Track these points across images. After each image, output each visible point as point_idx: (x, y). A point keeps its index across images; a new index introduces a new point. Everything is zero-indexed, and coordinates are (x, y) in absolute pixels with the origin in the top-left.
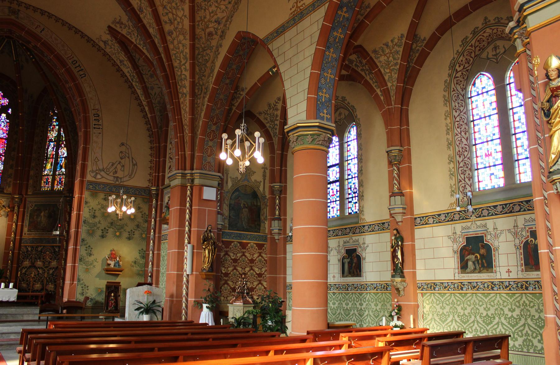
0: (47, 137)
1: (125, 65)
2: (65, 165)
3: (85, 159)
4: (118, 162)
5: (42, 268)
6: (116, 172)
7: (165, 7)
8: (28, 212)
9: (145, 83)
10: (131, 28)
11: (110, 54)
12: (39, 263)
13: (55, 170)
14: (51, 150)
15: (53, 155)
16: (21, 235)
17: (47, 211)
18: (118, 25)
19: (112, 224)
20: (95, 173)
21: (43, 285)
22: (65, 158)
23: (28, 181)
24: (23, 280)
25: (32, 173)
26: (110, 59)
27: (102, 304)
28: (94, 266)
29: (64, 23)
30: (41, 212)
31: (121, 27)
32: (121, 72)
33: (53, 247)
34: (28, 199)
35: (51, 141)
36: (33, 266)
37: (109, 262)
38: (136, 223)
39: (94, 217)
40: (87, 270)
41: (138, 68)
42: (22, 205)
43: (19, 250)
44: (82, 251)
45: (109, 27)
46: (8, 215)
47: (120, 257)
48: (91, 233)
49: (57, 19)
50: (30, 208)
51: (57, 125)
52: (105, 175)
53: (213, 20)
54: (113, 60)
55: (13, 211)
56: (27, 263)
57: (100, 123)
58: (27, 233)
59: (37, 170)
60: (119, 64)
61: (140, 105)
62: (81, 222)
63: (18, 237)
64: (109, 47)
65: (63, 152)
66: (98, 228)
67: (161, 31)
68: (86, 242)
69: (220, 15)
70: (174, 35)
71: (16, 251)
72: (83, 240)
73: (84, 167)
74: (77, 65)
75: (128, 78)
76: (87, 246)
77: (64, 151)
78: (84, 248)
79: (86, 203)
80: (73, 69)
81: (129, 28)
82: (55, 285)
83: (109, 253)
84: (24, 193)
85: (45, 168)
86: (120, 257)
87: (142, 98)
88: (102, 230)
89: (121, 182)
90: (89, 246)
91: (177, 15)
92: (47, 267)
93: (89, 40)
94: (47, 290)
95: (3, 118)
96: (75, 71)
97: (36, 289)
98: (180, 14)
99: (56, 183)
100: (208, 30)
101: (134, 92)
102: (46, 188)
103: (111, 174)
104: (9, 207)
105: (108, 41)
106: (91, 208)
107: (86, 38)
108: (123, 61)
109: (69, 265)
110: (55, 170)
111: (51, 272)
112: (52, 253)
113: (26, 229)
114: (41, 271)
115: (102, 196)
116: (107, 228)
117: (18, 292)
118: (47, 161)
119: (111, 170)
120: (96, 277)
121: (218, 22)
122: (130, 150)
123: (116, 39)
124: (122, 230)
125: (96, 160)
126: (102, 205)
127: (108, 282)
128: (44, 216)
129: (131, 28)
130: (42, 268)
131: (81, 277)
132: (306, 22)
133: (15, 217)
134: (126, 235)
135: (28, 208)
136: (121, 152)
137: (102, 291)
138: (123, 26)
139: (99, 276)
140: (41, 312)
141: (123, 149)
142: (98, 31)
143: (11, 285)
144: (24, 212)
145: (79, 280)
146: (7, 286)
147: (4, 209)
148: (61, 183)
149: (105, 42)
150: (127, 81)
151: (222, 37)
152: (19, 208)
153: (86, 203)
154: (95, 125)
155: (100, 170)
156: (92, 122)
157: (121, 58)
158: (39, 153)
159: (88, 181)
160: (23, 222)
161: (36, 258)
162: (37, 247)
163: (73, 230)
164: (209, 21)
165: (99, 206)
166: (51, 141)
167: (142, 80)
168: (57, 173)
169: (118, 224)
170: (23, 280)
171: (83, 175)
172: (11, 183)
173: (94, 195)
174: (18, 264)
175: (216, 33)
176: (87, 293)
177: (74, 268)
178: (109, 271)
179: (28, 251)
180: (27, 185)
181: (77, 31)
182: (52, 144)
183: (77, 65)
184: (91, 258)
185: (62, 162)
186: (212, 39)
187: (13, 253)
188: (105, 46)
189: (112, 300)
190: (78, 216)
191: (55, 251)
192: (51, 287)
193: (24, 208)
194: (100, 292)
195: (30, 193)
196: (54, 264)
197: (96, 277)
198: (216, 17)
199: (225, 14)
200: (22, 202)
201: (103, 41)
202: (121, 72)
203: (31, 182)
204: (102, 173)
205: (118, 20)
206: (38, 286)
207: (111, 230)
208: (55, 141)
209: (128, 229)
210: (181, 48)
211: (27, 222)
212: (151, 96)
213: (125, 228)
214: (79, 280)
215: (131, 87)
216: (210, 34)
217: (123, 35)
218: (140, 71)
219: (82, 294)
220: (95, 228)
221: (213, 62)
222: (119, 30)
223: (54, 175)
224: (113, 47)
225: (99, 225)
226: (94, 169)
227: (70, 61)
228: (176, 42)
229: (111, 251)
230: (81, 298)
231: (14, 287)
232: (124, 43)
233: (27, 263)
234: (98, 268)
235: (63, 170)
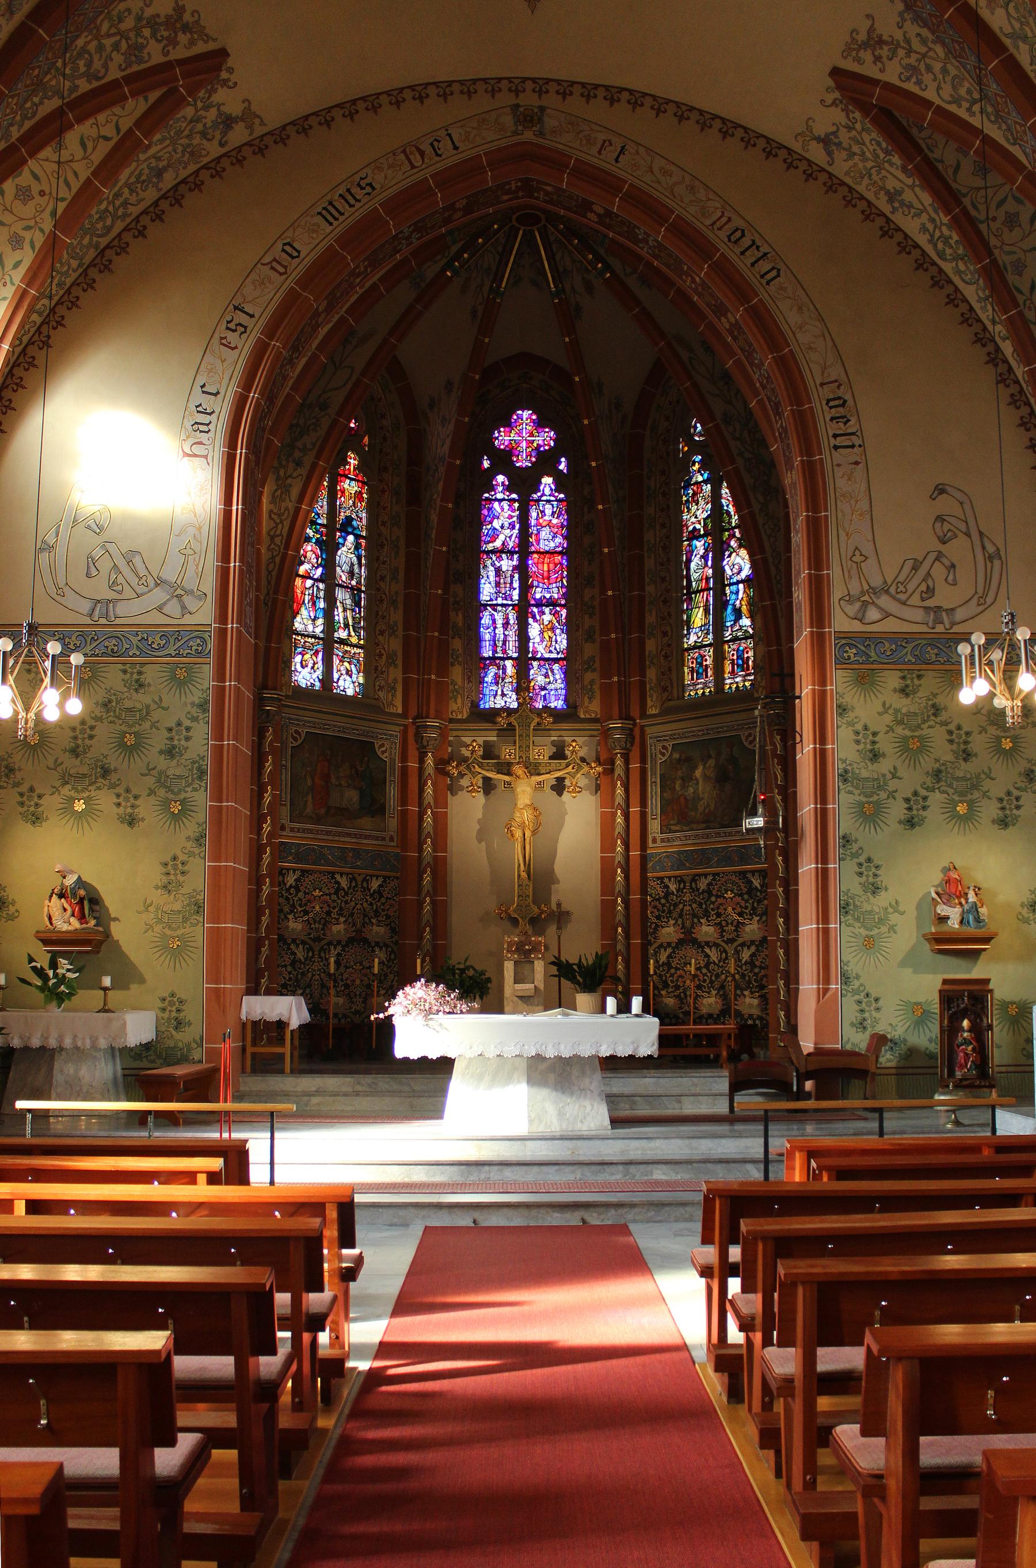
0: (681, 525)
1: (910, 206)
2: (749, 604)
3: (818, 559)
4: (932, 557)
5: (716, 945)
6: (930, 592)
8: (654, 774)
9: (990, 254)
10: (916, 45)
11: (848, 180)
12: (706, 931)
13: (719, 626)
14: (698, 568)
15: (707, 579)
16: (644, 846)
17: (711, 762)
18: (867, 56)
19: (937, 774)
20: (858, 605)
21: (725, 997)
22: (747, 581)
23: (643, 674)
24: (666, 985)
25: (651, 645)
26: (852, 198)
27: (931, 1056)
28: (892, 929)
29: (683, 112)
30: (696, 768)
31: (878, 59)
32: (899, 237)
33: (743, 874)
34: (648, 730)
35: (694, 535)
36: (688, 939)
37: (942, 910)
38: (1023, 765)
39: (875, 756)
40: (869, 944)
41: (959, 203)
42: (635, 754)
43: (644, 891)
44: (846, 879)
45: (836, 72)
46: (598, 788)
47: (978, 890)
48: (870, 814)
49: (660, 105)
50: (659, 757)
51: (705, 482)
52: (892, 606)
54: (862, 198)
55: (612, 771)
56: (669, 932)
57: (852, 426)
58: (659, 836)
59: (665, 634)
60: (886, 209)
61: (983, 338)
62: (833, 779)
63: (635, 853)
64: (844, 154)
65: (739, 563)
66: (892, 795)
68: (855, 847)
71: (635, 897)
72: (846, 840)
73: (818, 588)
74: (746, 242)
75: (924, 253)
76: (862, 859)
77: (738, 560)
78: (850, 867)
79: (842, 710)
80: (734, 258)
81: (910, 51)
82: (764, 998)
83: (938, 877)
84: (635, 711)
85: (688, 623)
86: (978, 890)
87: (986, 313)
88: (907, 800)
89: (953, 624)
90: (869, 860)
92: (730, 941)
93: (772, 148)
94: (738, 1014)
95: (547, 491)
96: (743, 264)
97: (704, 1010)
99: (728, 668)
101: (955, 299)
102: (698, 687)
103: (915, 600)
104: (598, 760)
106: (859, 727)
107: (761, 143)
108: (900, 193)
109: (807, 927)
110: (719, 626)
111: (746, 955)
112: (741, 895)
113: (654, 826)
114: (714, 955)
115: (892, 680)
116: (923, 792)
117: (661, 1024)
118: (690, 600)
119: (911, 587)
120: (904, 963)
122: (967, 507)
123: (865, 109)
124: (976, 795)
125: (858, 558)
126: (897, 711)
127: (945, 982)
128: (706, 777)
129: (916, 45)
130: (716, 945)
131: (853, 968)
133: (620, 791)
134: (990, 810)
135: (654, 760)
136: (940, 519)
137: (926, 1014)
138: (884, 51)
139: (910, 960)
140: (735, 1087)
141: (946, 505)
142: (797, 105)
143: (637, 1002)
144: (643, 772)
145: (846, 979)
146: (624, 1008)
147: (586, 769)
148: (745, 666)
149: (826, 141)
150: (923, 262)
152: (627, 762)
153: (842, 710)
154: (835, 436)
155: (874, 591)
156: (826, 428)
157: (891, 184)
158: (663, 580)
159: (841, 635)
160: (643, 803)
161: (694, 916)
162: (694, 879)
163: (807, 810)
165: (888, 719)
166: (694, 535)
167: (976, 243)
168: (728, 635)
169: (960, 774)
170: (666, 985)
171: (819, 615)
172: (596, 688)
173: (865, 680)
174: (644, 935)
176: (876, 1021)
177: (824, 936)
178: (946, 943)
179: (668, 894)
180: (642, 684)
181: (728, 128)
182: (699, 545)
183: (746, 242)
184: (882, 900)
185: (739, 596)
187: (626, 902)
188: (830, 154)
189: (966, 1042)
190: (821, 758)
191: (751, 890)
192: (749, 1004)
193: (643, 760)
194: (919, 1015)
195: (654, 711)
196: (752, 929)
197: (904, 963)
200: (635, 741)
201: (818, 139)
202: (899, 237)
203: (651, 674)
204: (884, 601)
205: (862, 37)
206: (710, 1002)
207: (936, 799)
208: (705, 535)
209: (997, 789)
211: (654, 805)
212: (1021, 299)
213: (987, 784)
214: (846, 979)
215: (940, 280)
217: (888, 86)
218: (965, 212)
219: (862, 1025)
220: (883, 795)
222: (871, 71)
223: (718, 644)
224: (856, 149)
225: (892, 785)
226: (855, 588)
227: (723, 235)
229: (946, 870)
230: (858, 1041)
231: (646, 1009)
233: (669, 932)
234: (906, 934)
235: (746, 622)
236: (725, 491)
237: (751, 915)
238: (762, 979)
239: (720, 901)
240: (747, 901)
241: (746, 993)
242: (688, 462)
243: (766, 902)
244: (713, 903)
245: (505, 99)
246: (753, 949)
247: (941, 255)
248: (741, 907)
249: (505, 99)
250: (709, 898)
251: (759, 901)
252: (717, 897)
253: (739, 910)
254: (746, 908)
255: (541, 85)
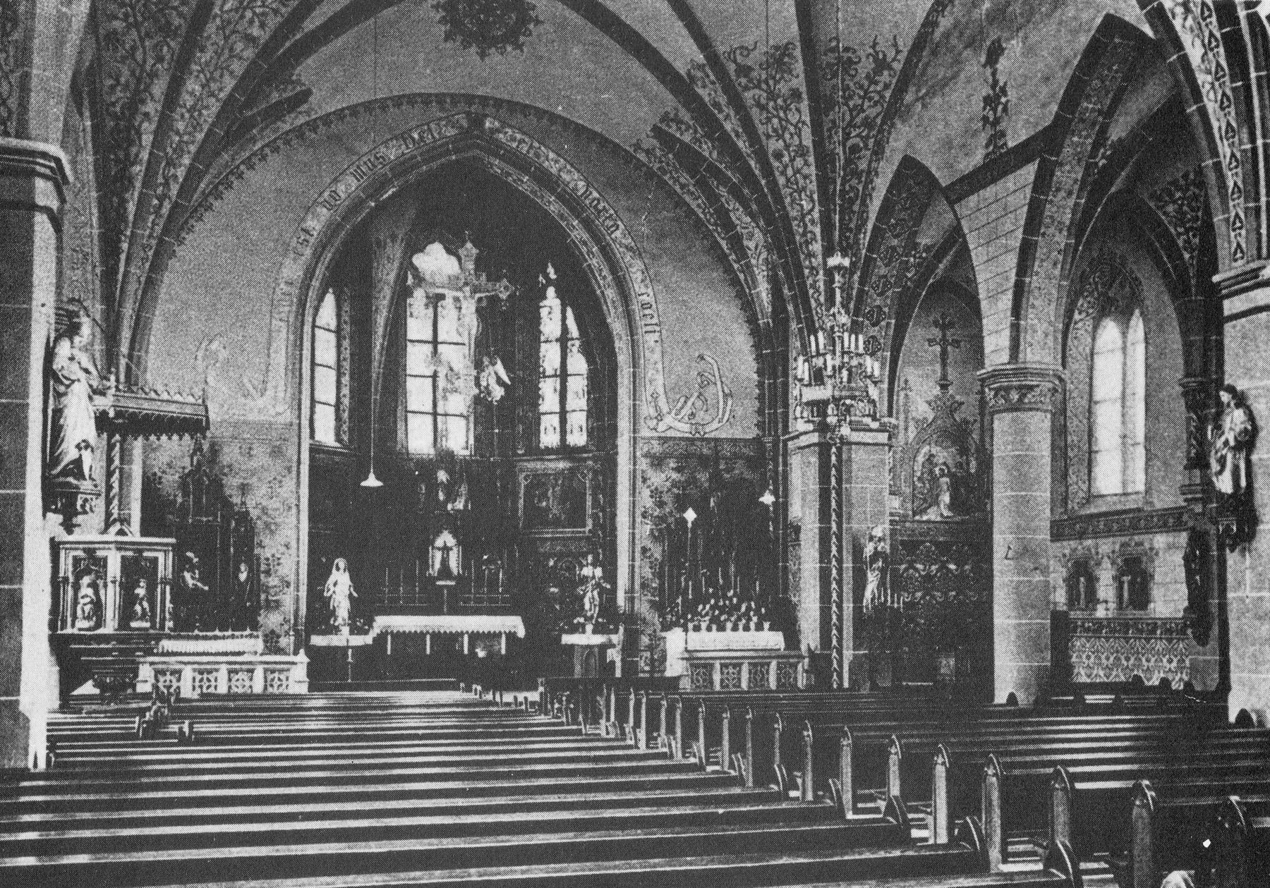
7: (763, 108)
53: (858, 120)
65: (578, 363)
67: (761, 155)
69: (872, 112)
70: (786, 159)
91: (787, 121)
98: (793, 118)
100: (849, 143)
105: (654, 149)
121: (868, 124)
132: (1010, 182)
149: (648, 152)
151: (878, 152)
157: (682, 180)
164: (850, 124)
175: (866, 146)
186: (859, 158)
198: (863, 115)
199: (879, 109)
210: (801, 182)
216: (855, 149)
221: (864, 204)
228: (790, 172)
232: (689, 159)
236: (569, 312)
242: (545, 288)
245: (462, 106)
247: (708, 221)
249: (462, 106)
255: (484, 100)
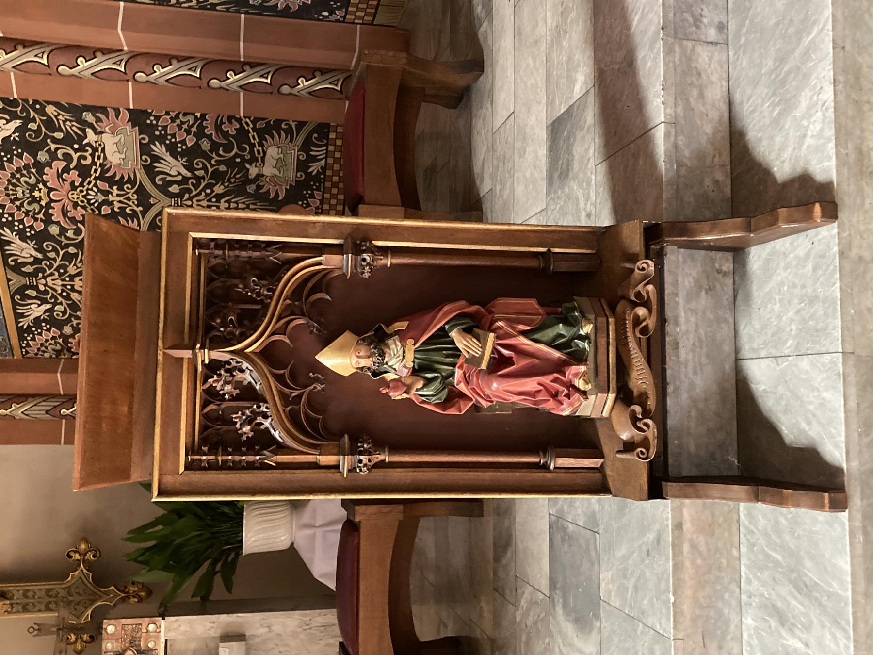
82: (270, 129)
111: (173, 167)
112: (40, 167)
237: (82, 149)
238: (226, 135)
239: (57, 216)
240: (53, 156)
241: (253, 171)
243: (51, 110)
244: (63, 231)
246: (159, 149)
248: (66, 170)
250: (51, 238)
251: (50, 124)
252: (48, 221)
253: (74, 175)
254: (67, 157)
